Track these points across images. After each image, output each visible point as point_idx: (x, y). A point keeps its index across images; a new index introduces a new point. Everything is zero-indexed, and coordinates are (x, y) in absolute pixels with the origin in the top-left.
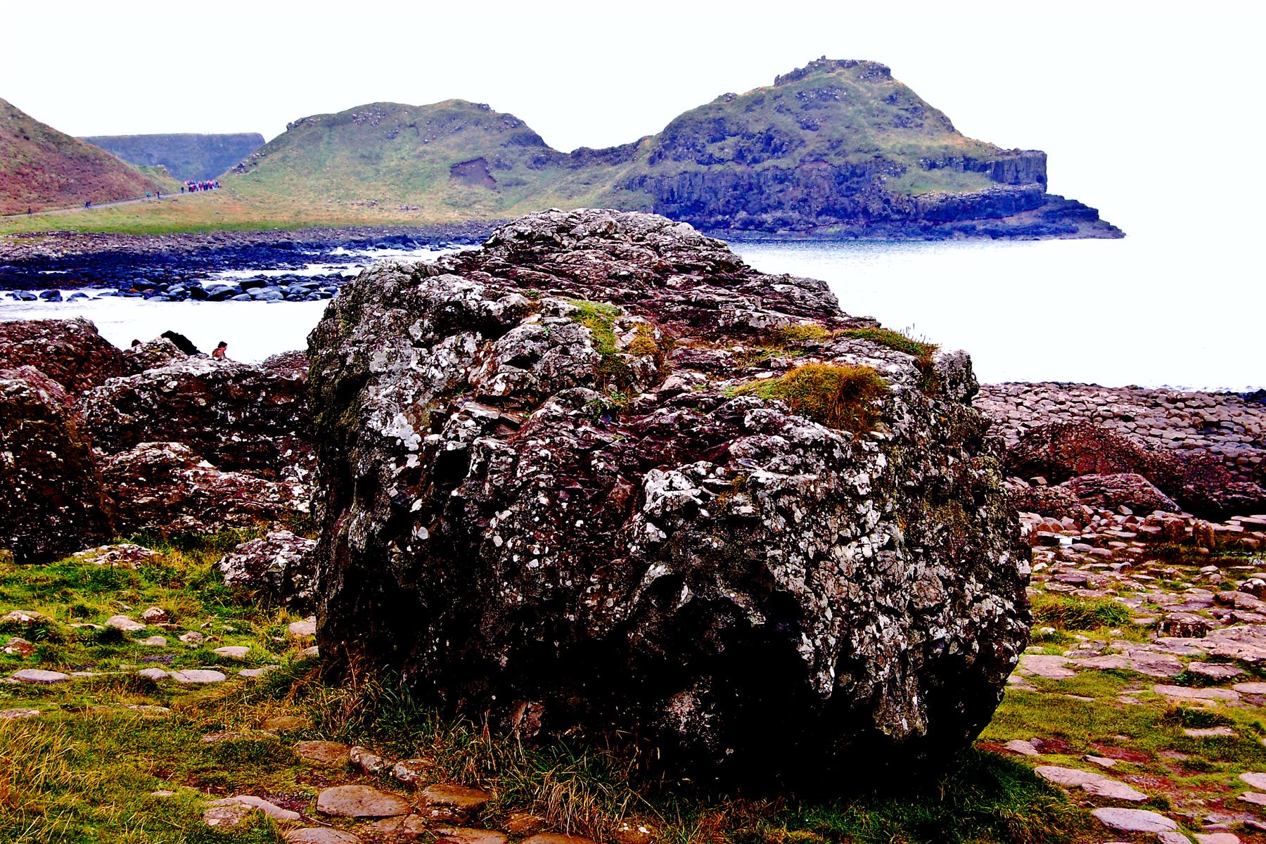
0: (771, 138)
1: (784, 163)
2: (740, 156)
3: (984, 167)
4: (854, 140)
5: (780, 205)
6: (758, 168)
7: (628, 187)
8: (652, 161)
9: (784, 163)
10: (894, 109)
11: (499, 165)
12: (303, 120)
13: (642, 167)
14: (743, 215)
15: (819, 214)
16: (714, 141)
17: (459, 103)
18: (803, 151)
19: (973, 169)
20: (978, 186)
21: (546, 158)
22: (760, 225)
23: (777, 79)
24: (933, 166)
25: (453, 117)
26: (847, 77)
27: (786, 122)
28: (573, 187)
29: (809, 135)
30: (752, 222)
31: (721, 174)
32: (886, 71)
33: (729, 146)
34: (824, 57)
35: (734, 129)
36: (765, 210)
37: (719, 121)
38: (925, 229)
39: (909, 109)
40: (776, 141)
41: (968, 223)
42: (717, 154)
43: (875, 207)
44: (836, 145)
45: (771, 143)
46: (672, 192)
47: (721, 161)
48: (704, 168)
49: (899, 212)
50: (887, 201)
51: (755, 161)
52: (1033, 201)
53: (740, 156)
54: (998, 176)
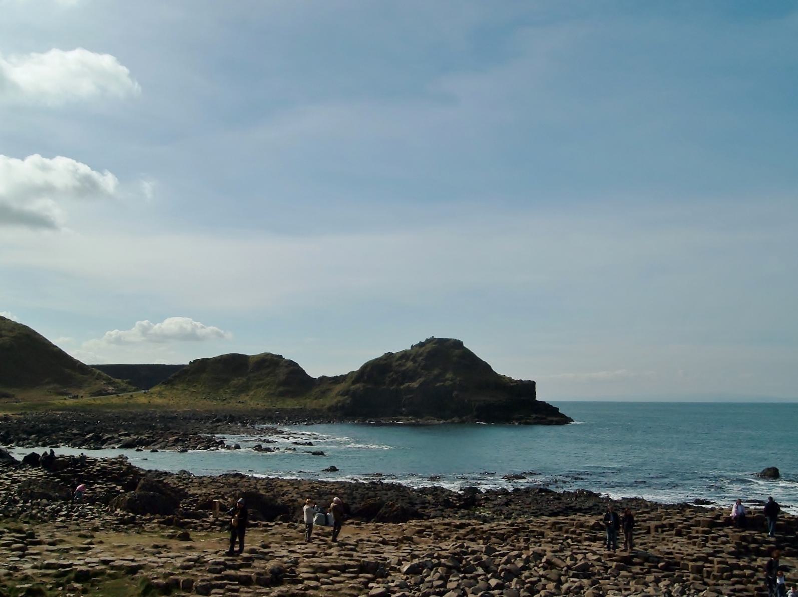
6: (402, 387)
7: (342, 395)
8: (354, 383)
18: (421, 379)
23: (412, 346)
34: (433, 336)
45: (408, 376)
51: (402, 384)
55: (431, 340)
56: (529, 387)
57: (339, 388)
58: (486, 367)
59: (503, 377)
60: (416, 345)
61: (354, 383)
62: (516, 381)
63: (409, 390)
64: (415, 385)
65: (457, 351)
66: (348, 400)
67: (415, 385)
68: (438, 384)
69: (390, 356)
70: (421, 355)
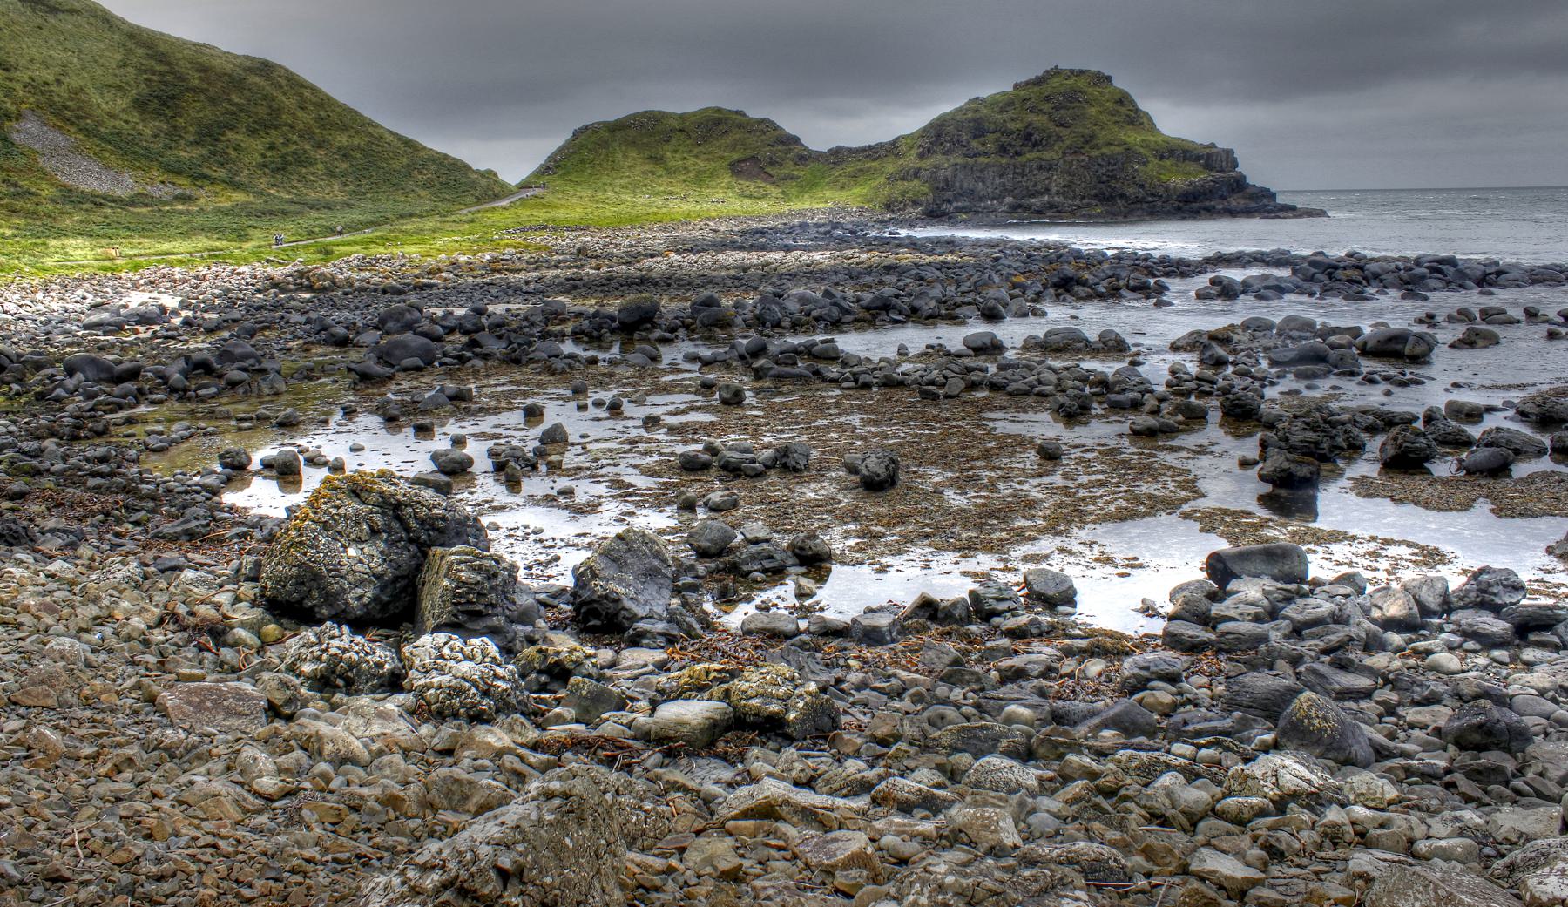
0: (1030, 134)
1: (1047, 155)
2: (1003, 150)
3: (1198, 158)
4: (1103, 136)
5: (1047, 190)
6: (1022, 159)
7: (903, 179)
9: (1047, 155)
10: (1123, 109)
11: (772, 163)
12: (587, 127)
13: (911, 160)
14: (1009, 199)
15: (1083, 198)
16: (975, 137)
17: (719, 110)
19: (1190, 159)
21: (806, 157)
22: (1027, 208)
23: (1016, 85)
25: (718, 122)
26: (1081, 83)
27: (1038, 120)
28: (842, 180)
29: (1064, 132)
30: (1020, 206)
31: (988, 165)
35: (992, 127)
36: (1033, 196)
38: (1179, 209)
40: (1036, 137)
41: (1207, 203)
42: (981, 148)
43: (1131, 191)
44: (1089, 139)
46: (946, 181)
47: (985, 154)
48: (971, 161)
49: (1152, 195)
50: (1142, 186)
51: (1018, 154)
52: (1239, 185)
54: (1209, 166)
60: (1027, 83)
61: (921, 156)
63: (1047, 167)
68: (1095, 153)
70: (1048, 99)
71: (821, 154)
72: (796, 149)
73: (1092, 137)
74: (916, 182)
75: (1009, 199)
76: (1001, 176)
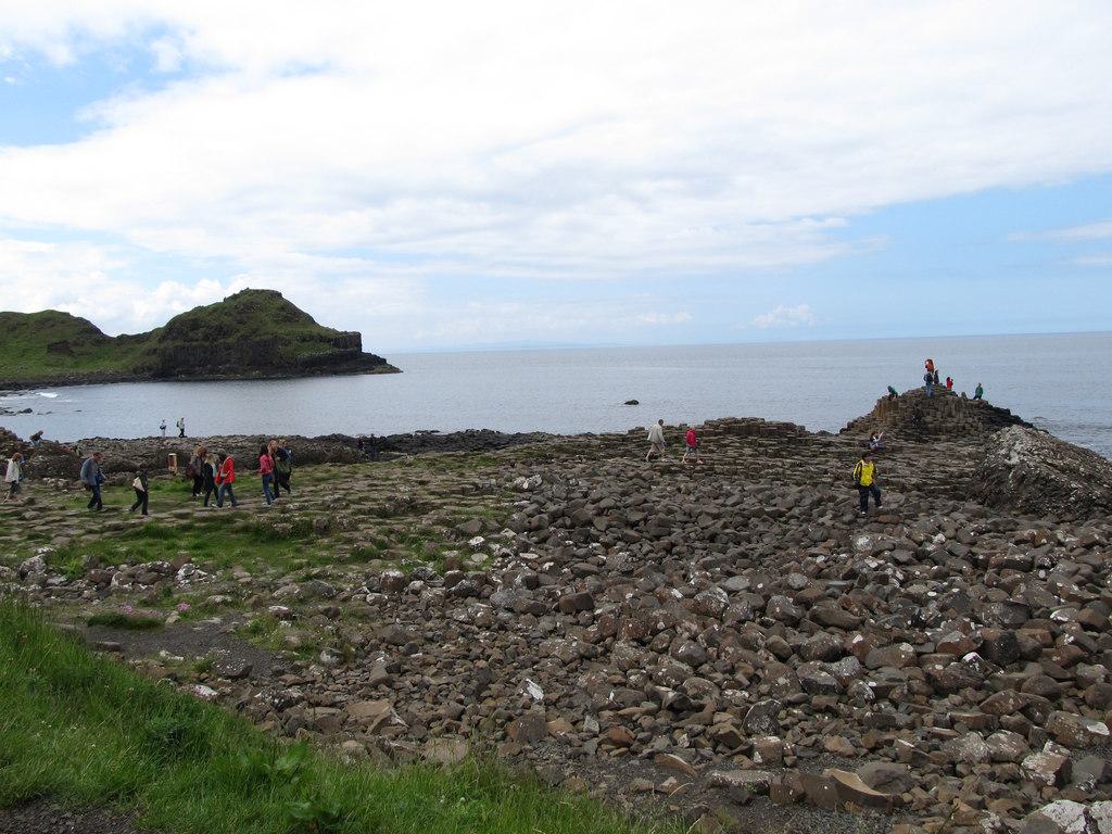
8: (160, 341)
11: (76, 344)
13: (153, 344)
14: (209, 366)
16: (192, 330)
20: (328, 350)
24: (304, 340)
25: (48, 320)
29: (241, 327)
32: (280, 295)
33: (200, 333)
37: (195, 320)
39: (290, 314)
45: (222, 331)
47: (197, 340)
51: (215, 340)
53: (206, 338)
55: (247, 292)
56: (354, 339)
57: (146, 346)
58: (309, 320)
59: (328, 330)
62: (342, 333)
63: (228, 348)
64: (231, 340)
65: (278, 304)
66: (154, 360)
67: (231, 340)
68: (258, 339)
69: (199, 309)
71: (111, 339)
72: (95, 336)
73: (257, 330)
74: (153, 357)
75: (209, 366)
76: (205, 353)
